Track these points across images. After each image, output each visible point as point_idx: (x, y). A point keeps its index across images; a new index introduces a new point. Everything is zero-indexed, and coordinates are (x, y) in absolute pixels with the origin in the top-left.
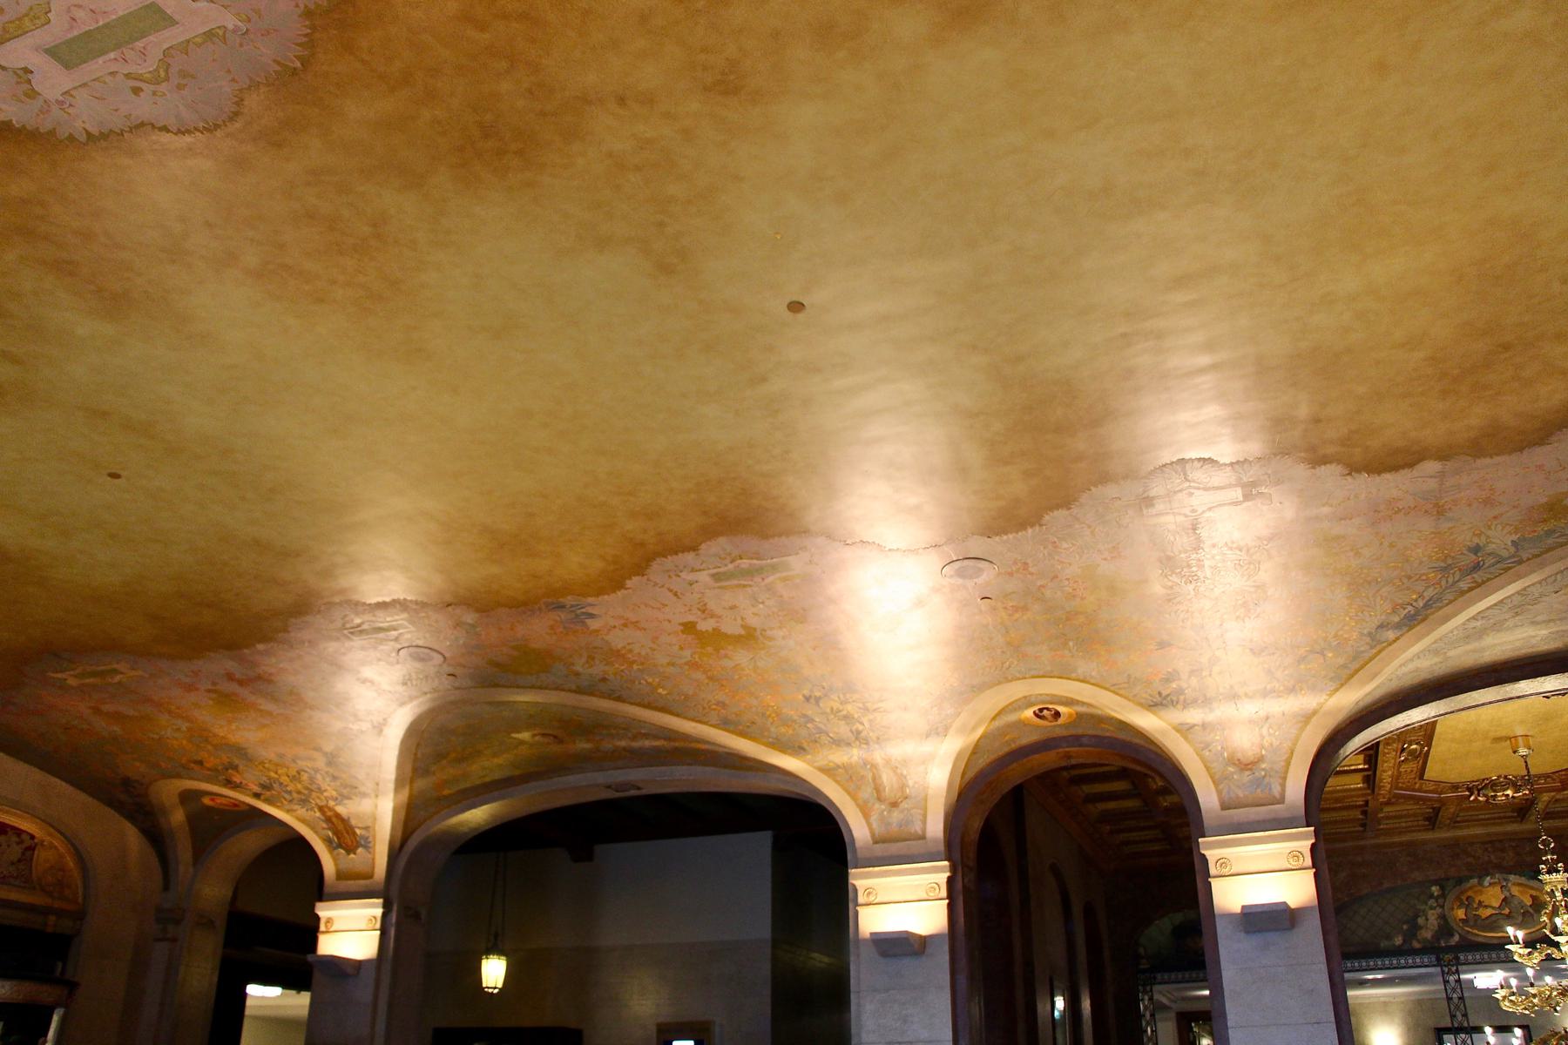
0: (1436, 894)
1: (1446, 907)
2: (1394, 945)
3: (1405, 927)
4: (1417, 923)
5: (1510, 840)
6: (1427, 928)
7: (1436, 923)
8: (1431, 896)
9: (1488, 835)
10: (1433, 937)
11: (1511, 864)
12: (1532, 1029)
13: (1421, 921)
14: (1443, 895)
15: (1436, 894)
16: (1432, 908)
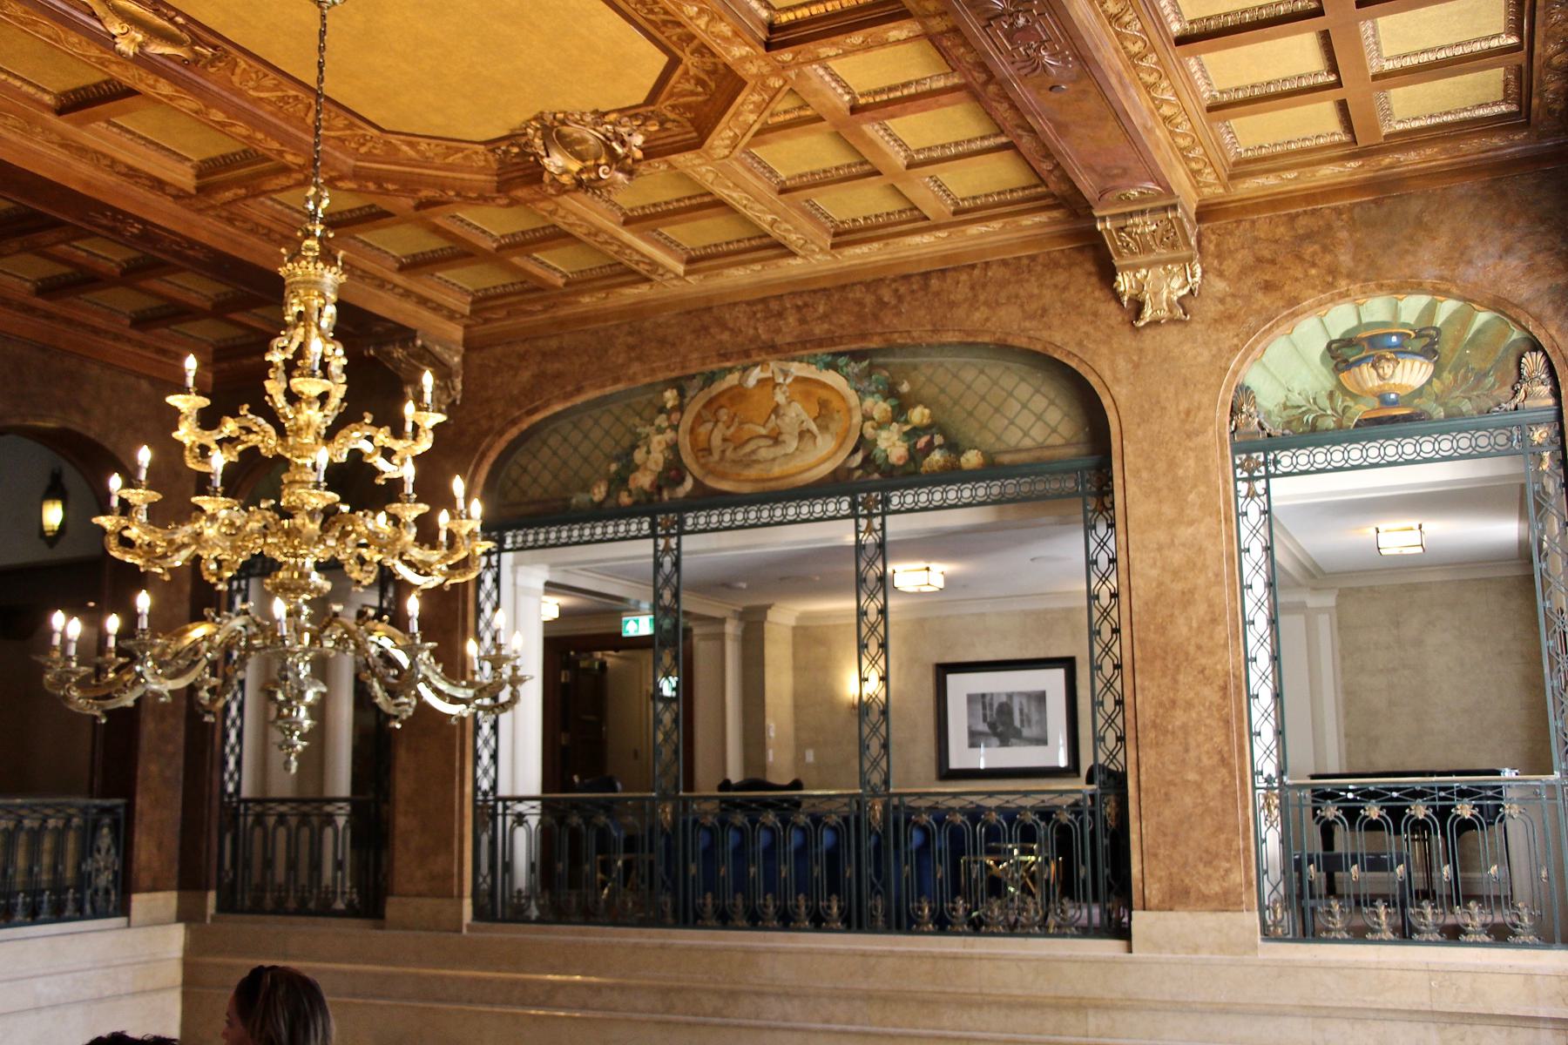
0: (669, 405)
1: (681, 429)
2: (592, 501)
3: (614, 467)
4: (632, 460)
5: (794, 294)
6: (646, 469)
7: (660, 458)
8: (662, 409)
9: (762, 285)
10: (652, 485)
11: (789, 339)
12: (950, 659)
13: (639, 456)
14: (680, 408)
15: (669, 405)
16: (660, 431)
